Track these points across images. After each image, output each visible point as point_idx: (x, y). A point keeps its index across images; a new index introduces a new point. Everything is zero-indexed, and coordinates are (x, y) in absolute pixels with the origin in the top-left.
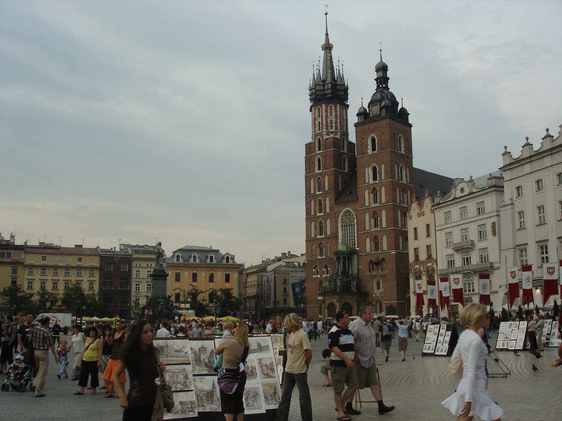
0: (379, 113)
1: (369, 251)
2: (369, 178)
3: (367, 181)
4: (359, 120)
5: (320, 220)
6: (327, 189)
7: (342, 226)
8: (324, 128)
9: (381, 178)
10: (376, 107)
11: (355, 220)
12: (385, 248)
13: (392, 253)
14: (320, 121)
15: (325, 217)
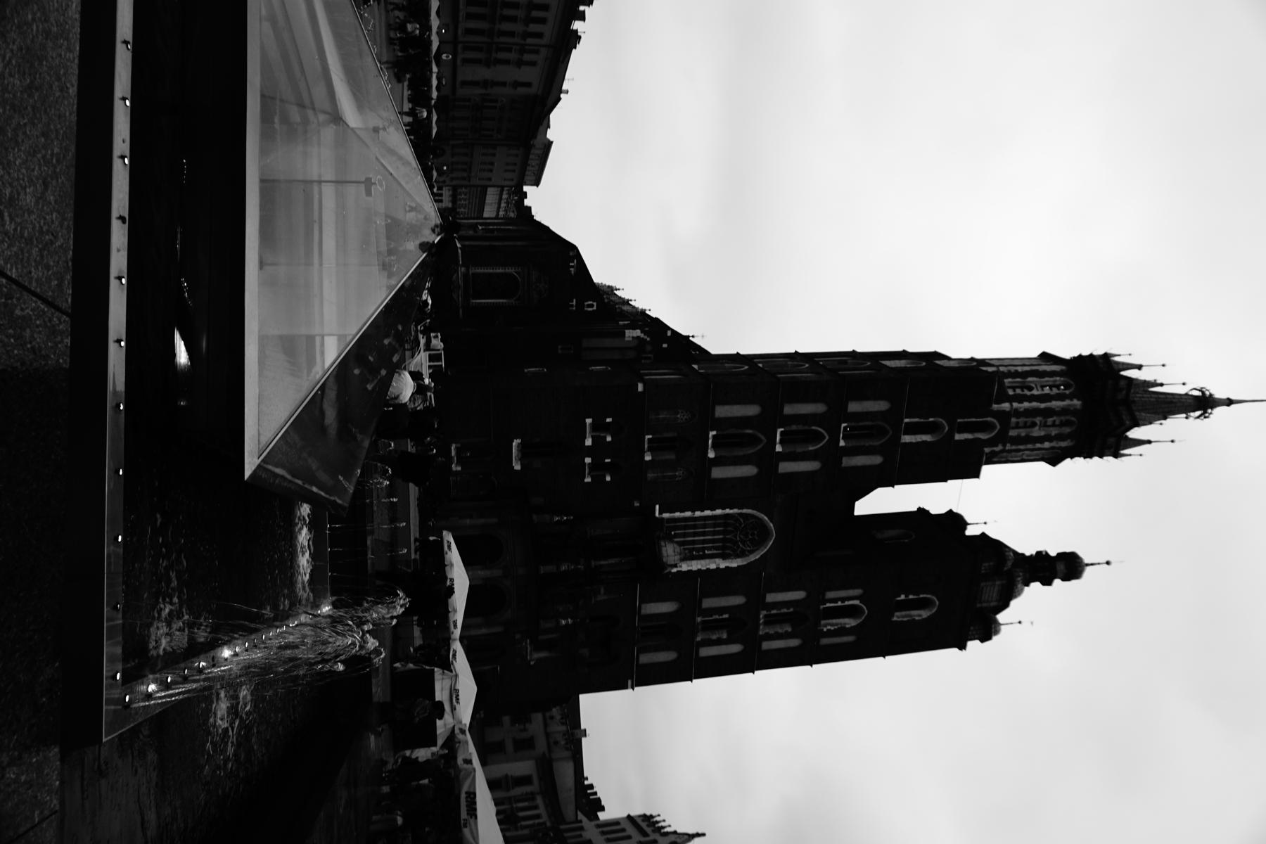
0: (978, 605)
1: (643, 612)
2: (835, 601)
3: (830, 595)
4: (987, 564)
5: (761, 441)
6: (848, 462)
7: (727, 515)
8: (1014, 447)
9: (825, 637)
10: (995, 595)
11: (734, 565)
12: (645, 659)
13: (630, 682)
14: (1036, 432)
15: (767, 460)
